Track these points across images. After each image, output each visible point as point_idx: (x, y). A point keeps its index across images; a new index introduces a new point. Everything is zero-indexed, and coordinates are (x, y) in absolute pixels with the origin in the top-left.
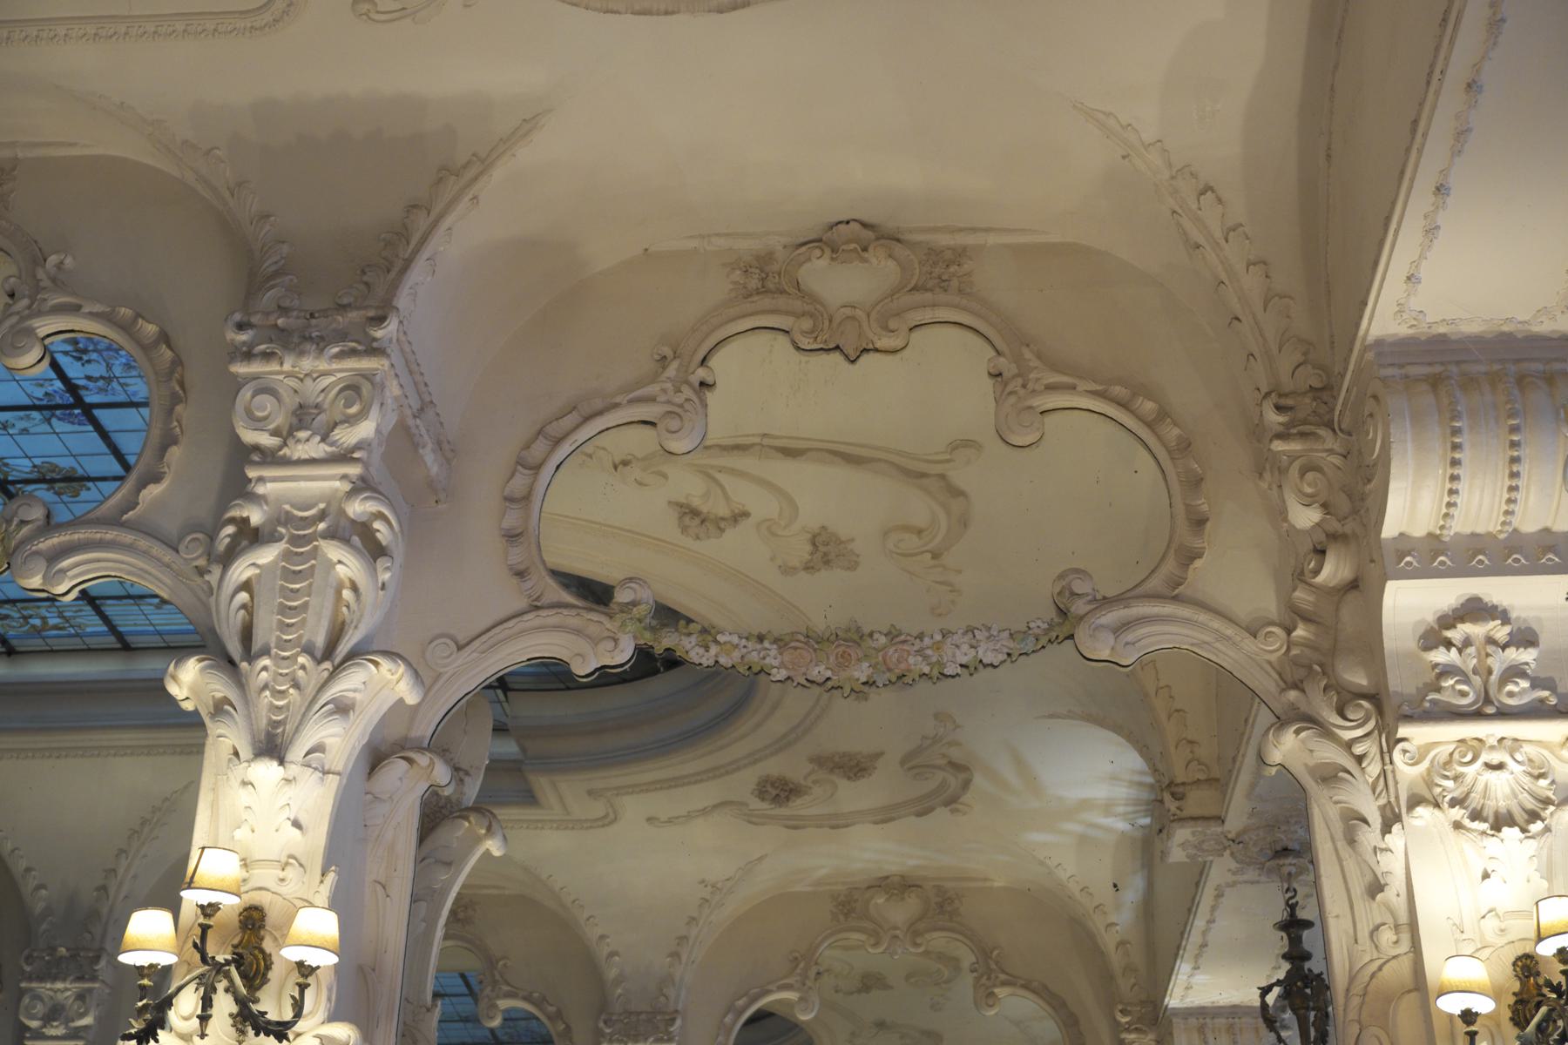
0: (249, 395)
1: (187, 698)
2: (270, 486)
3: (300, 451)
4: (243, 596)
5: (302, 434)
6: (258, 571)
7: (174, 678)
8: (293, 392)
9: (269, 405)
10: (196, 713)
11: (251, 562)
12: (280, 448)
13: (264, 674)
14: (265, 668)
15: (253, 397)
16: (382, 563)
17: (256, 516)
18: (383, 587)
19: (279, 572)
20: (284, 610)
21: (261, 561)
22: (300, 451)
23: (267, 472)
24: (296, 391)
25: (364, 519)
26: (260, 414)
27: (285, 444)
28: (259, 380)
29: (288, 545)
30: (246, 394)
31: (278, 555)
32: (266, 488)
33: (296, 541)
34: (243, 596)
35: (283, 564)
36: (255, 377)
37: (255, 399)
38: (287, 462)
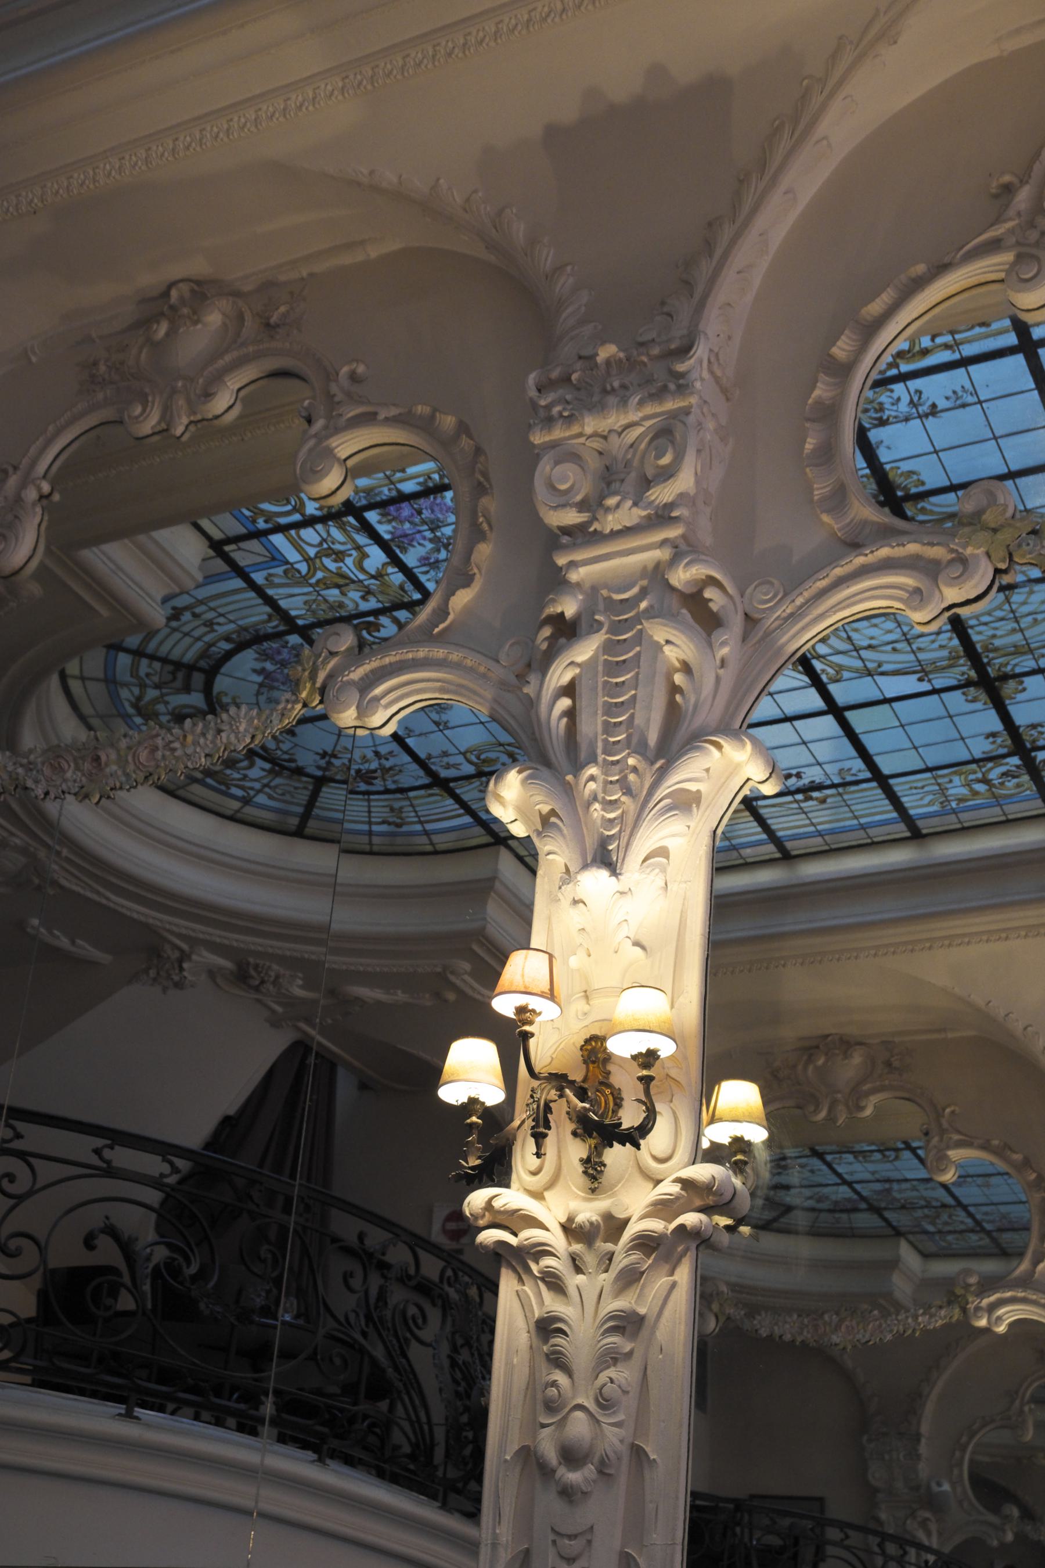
0: (548, 468)
1: (516, 820)
2: (583, 571)
3: (611, 522)
4: (565, 703)
5: (611, 501)
6: (577, 671)
7: (499, 798)
8: (597, 454)
9: (571, 474)
10: (529, 837)
11: (569, 661)
12: (589, 523)
13: (592, 785)
14: (592, 778)
15: (552, 470)
16: (721, 635)
17: (569, 607)
18: (723, 663)
19: (600, 668)
20: (611, 709)
21: (580, 659)
22: (611, 522)
23: (579, 556)
24: (600, 453)
25: (694, 590)
26: (563, 487)
27: (595, 519)
28: (558, 448)
29: (608, 636)
30: (545, 467)
31: (598, 648)
32: (579, 573)
33: (617, 628)
34: (565, 703)
35: (606, 657)
36: (554, 445)
37: (554, 471)
38: (599, 537)
